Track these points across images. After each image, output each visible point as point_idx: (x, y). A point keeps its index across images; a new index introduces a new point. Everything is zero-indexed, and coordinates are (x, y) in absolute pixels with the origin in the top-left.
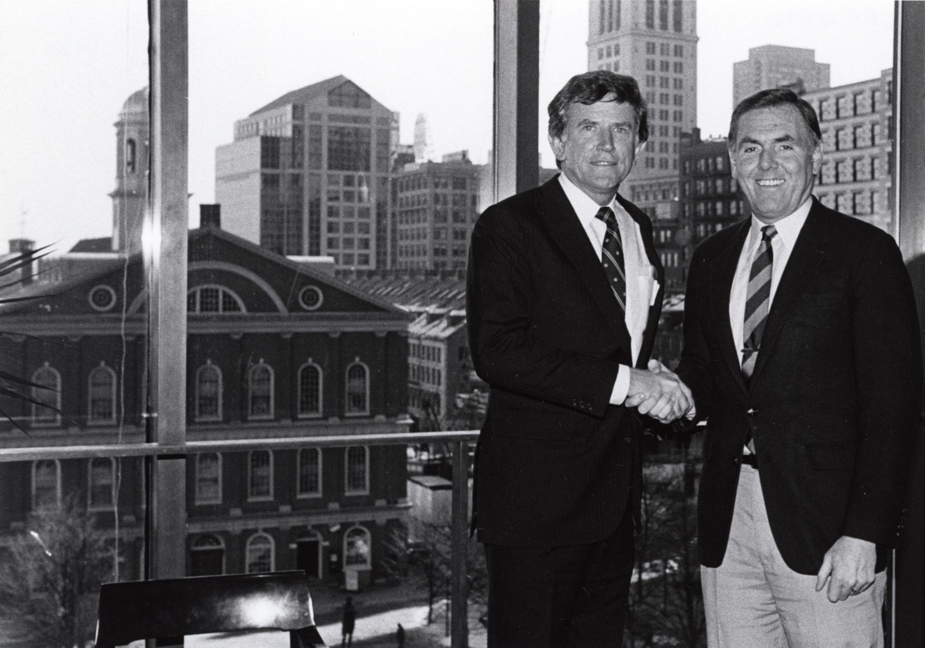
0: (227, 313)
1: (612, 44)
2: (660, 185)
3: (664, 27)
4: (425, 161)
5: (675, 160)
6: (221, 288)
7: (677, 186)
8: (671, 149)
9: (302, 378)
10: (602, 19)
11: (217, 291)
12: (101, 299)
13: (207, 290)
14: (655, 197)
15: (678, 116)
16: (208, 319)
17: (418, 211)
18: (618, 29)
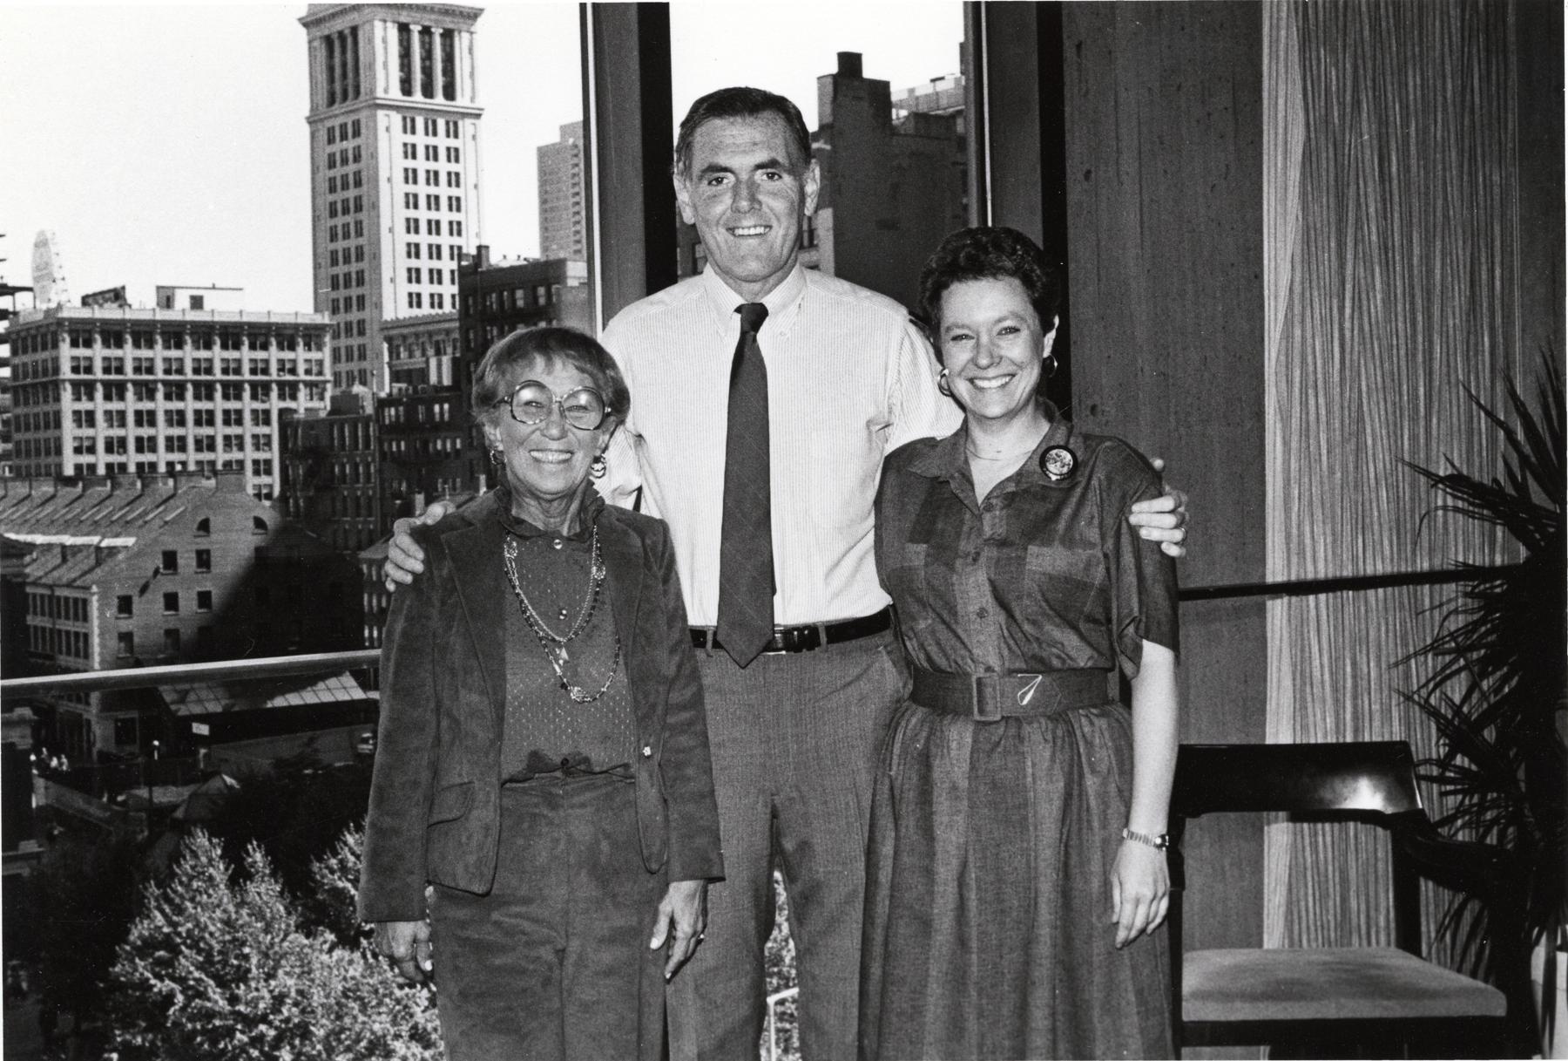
1: (349, 120)
2: (430, 334)
3: (428, 91)
4: (53, 305)
5: (453, 296)
7: (456, 335)
8: (446, 277)
10: (331, 80)
14: (424, 354)
15: (456, 228)
17: (45, 385)
18: (357, 93)
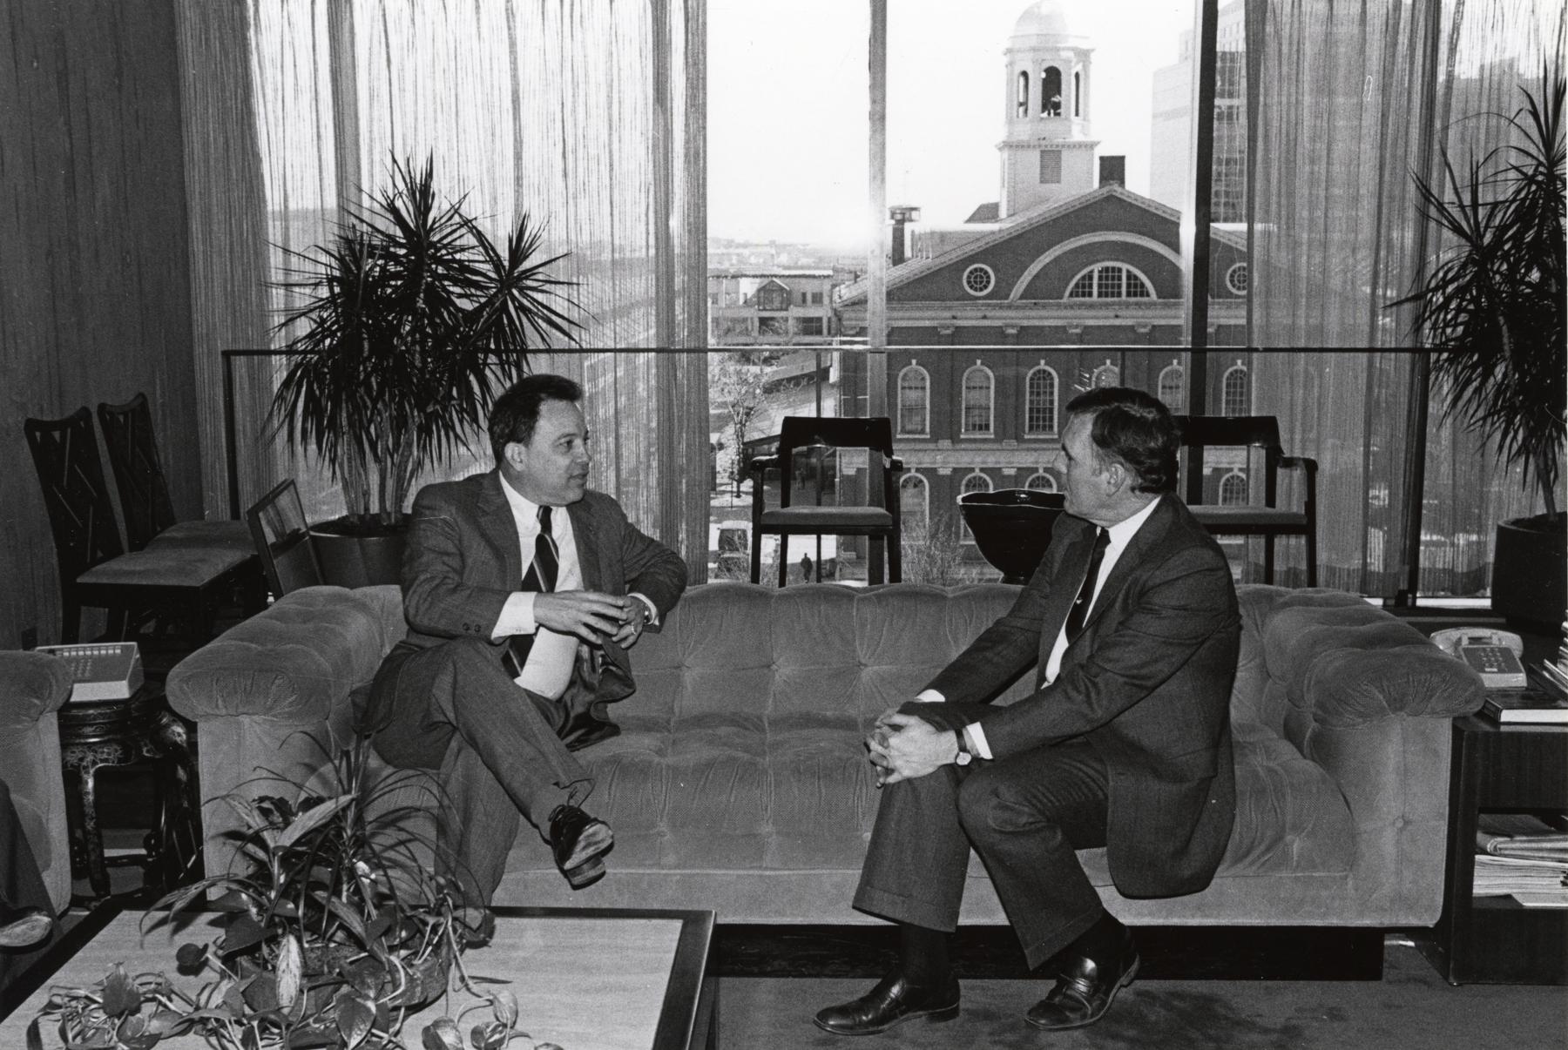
0: (1133, 299)
6: (1125, 267)
9: (1228, 385)
11: (1120, 270)
12: (979, 280)
13: (1107, 269)
16: (1107, 305)
